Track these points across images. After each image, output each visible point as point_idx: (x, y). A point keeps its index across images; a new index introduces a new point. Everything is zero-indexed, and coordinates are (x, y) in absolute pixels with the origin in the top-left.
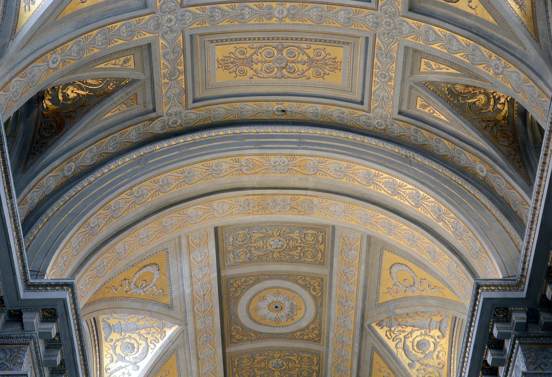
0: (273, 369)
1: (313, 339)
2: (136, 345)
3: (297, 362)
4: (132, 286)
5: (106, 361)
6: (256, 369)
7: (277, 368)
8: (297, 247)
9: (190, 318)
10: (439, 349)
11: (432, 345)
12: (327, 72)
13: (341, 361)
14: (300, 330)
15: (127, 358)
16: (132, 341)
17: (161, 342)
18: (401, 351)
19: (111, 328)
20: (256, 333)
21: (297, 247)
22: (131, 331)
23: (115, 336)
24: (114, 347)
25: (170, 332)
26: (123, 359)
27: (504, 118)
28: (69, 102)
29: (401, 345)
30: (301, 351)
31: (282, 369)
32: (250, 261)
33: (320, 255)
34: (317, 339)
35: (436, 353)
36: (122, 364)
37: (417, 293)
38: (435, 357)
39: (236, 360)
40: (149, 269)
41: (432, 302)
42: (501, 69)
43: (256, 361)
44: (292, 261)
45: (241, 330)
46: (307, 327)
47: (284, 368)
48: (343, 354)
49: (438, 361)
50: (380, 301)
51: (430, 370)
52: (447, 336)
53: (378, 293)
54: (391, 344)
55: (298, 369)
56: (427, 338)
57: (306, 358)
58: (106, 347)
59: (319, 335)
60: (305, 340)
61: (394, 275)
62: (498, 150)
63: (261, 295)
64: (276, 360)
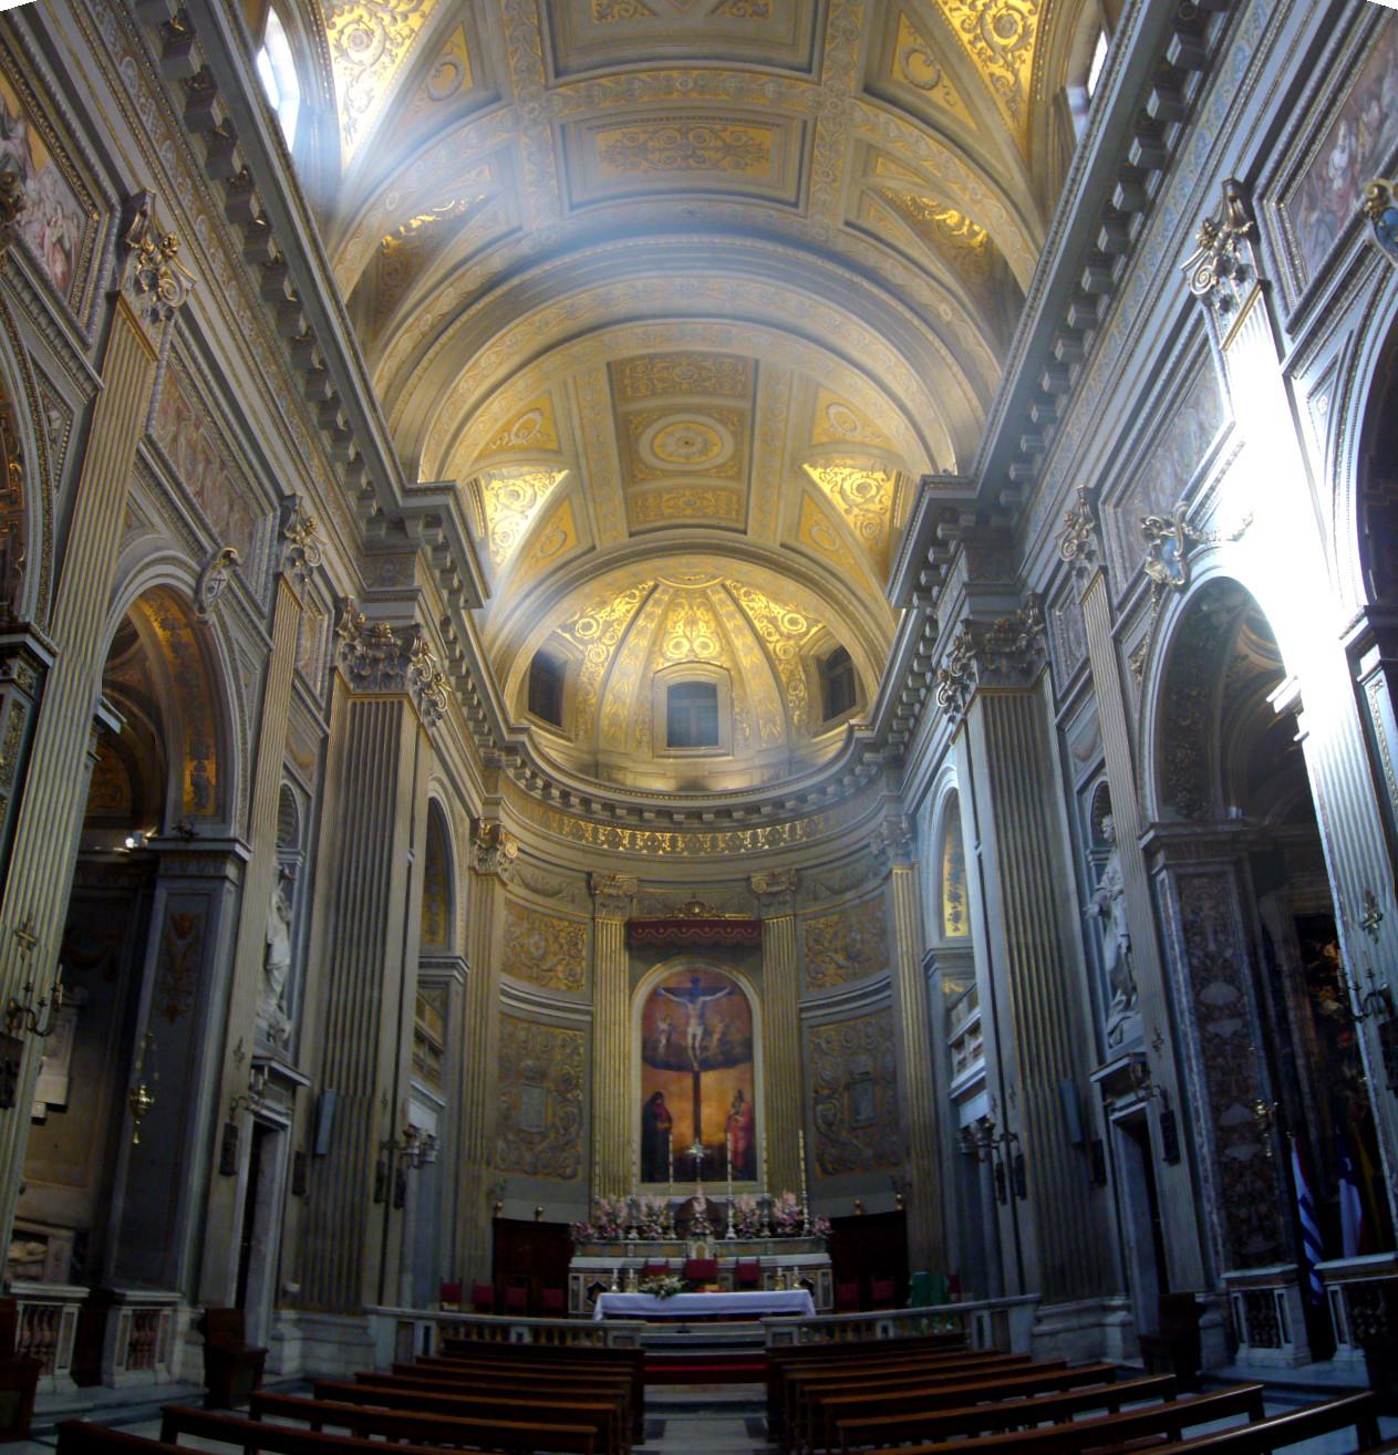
2: (521, 492)
4: (513, 437)
5: (489, 511)
8: (710, 378)
9: (583, 462)
10: (882, 492)
11: (874, 489)
12: (750, 162)
14: (716, 467)
15: (513, 507)
16: (517, 488)
17: (551, 488)
18: (839, 497)
19: (491, 477)
20: (662, 471)
21: (710, 378)
22: (514, 478)
23: (496, 484)
24: (497, 496)
25: (560, 477)
26: (508, 507)
27: (981, 244)
28: (413, 234)
29: (837, 489)
32: (654, 394)
33: (740, 386)
34: (738, 477)
36: (509, 513)
37: (858, 438)
38: (877, 500)
40: (530, 415)
41: (876, 452)
42: (979, 197)
44: (705, 392)
46: (725, 464)
50: (814, 442)
51: (870, 515)
52: (893, 480)
53: (811, 433)
54: (826, 488)
56: (869, 481)
58: (488, 497)
59: (739, 473)
61: (832, 416)
62: (968, 291)
63: (669, 430)
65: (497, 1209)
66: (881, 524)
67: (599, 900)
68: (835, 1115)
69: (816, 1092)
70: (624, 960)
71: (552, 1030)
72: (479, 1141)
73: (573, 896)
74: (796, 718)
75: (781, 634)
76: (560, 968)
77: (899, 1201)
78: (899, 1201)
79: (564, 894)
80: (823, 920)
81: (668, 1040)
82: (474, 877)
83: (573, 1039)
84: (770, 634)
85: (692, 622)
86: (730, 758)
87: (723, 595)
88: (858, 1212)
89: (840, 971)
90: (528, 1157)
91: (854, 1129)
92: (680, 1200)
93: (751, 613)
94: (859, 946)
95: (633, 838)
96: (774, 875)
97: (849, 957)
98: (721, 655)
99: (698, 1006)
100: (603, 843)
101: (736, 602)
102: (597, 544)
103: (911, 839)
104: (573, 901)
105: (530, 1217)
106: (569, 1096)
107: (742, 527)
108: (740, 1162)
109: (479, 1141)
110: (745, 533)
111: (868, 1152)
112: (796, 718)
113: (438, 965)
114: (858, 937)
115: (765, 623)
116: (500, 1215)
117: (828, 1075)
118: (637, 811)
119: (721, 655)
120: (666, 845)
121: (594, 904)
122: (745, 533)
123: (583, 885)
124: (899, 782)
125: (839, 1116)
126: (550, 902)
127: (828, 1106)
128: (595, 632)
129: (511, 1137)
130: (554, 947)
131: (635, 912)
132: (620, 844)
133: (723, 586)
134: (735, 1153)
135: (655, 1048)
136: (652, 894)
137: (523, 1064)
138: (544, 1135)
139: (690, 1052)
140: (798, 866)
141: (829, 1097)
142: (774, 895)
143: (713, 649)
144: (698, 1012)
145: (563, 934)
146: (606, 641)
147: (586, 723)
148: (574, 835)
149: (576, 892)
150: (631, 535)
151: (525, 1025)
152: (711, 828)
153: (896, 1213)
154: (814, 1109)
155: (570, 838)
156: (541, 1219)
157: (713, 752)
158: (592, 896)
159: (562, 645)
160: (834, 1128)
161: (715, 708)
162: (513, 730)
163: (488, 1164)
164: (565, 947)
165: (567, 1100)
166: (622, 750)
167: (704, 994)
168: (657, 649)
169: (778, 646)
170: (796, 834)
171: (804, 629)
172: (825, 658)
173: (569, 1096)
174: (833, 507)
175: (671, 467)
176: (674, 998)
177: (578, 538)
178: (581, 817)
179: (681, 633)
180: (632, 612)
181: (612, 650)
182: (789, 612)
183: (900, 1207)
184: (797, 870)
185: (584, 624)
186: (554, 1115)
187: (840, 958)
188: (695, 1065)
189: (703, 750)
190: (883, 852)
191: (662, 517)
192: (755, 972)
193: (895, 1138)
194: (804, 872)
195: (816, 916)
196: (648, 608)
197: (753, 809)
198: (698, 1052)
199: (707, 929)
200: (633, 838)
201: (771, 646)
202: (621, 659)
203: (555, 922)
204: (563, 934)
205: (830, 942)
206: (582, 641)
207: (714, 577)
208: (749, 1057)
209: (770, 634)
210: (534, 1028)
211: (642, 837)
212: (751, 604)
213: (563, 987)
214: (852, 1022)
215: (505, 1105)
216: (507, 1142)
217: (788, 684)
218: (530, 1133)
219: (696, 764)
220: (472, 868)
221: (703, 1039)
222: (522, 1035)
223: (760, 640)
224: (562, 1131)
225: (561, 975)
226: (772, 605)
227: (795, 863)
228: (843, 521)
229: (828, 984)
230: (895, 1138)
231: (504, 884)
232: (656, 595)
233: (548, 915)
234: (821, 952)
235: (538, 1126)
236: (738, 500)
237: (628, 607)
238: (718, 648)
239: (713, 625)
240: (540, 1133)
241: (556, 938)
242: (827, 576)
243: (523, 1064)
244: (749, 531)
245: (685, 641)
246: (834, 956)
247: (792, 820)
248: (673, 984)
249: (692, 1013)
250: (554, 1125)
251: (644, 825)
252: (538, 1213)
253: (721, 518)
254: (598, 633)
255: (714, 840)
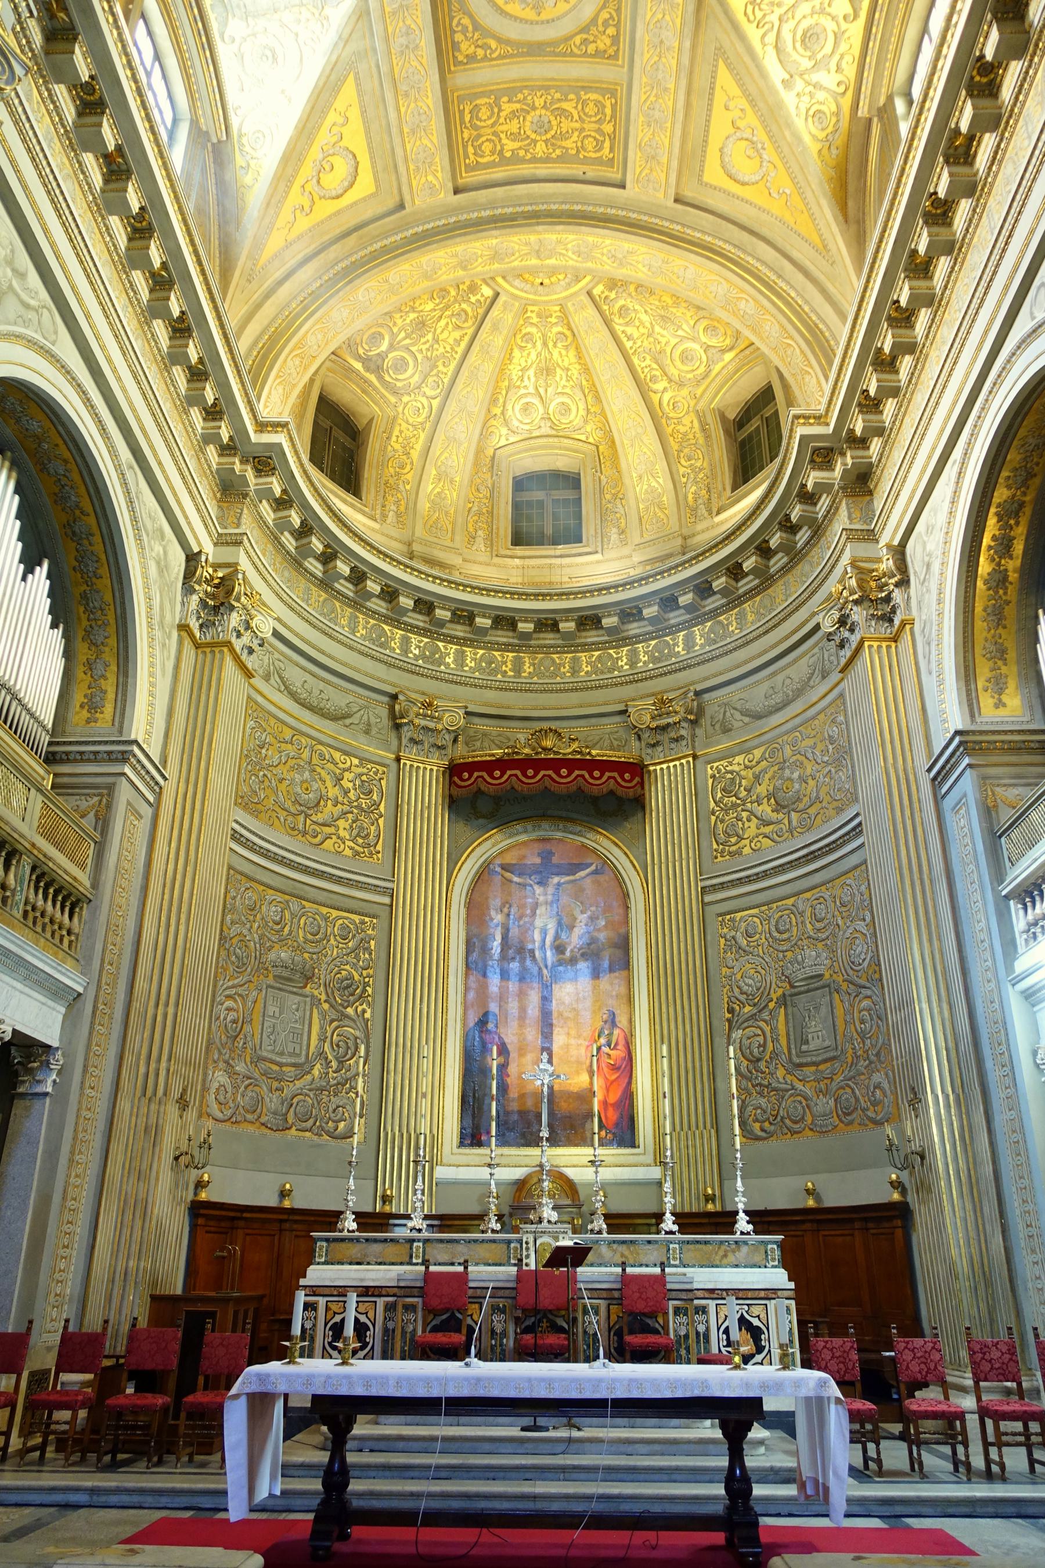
0: (533, 136)
1: (605, 51)
3: (576, 117)
6: (503, 136)
7: (540, 134)
10: (843, 47)
13: (656, 96)
18: (771, 51)
29: (771, 38)
30: (583, 88)
31: (549, 136)
35: (836, 57)
38: (833, 66)
39: (467, 111)
43: (503, 114)
45: (470, 28)
46: (594, 21)
47: (553, 132)
48: (660, 77)
49: (839, 77)
51: (821, 95)
54: (753, 34)
55: (576, 134)
57: (591, 105)
59: (615, 40)
60: (592, 56)
64: (538, 112)
65: (200, 1185)
66: (837, 114)
67: (407, 733)
68: (764, 1045)
69: (731, 1011)
70: (439, 820)
71: (324, 910)
72: (164, 1064)
73: (369, 725)
74: (690, 497)
75: (670, 381)
76: (341, 823)
77: (898, 1185)
78: (898, 1185)
79: (355, 719)
80: (739, 759)
81: (505, 938)
82: (187, 643)
83: (360, 928)
84: (654, 379)
85: (547, 371)
86: (598, 557)
87: (591, 311)
88: (811, 1203)
89: (767, 830)
90: (272, 1101)
91: (800, 1065)
92: (518, 1173)
93: (628, 344)
94: (797, 786)
95: (460, 658)
96: (663, 702)
97: (779, 807)
98: (586, 422)
99: (551, 890)
100: (416, 658)
101: (608, 323)
102: (407, 198)
103: (897, 585)
104: (367, 732)
105: (272, 1201)
106: (350, 1011)
107: (615, 175)
108: (612, 1115)
109: (164, 1064)
110: (624, 187)
111: (824, 1104)
112: (690, 497)
113: (95, 758)
114: (796, 775)
115: (648, 362)
116: (203, 1196)
117: (749, 985)
118: (464, 615)
119: (586, 422)
120: (508, 668)
121: (400, 739)
122: (624, 187)
123: (384, 712)
124: (868, 514)
125: (770, 1046)
126: (329, 727)
127: (749, 1031)
128: (411, 376)
129: (240, 1068)
130: (333, 792)
131: (461, 752)
132: (440, 662)
133: (589, 294)
134: (604, 1103)
135: (485, 950)
136: (485, 735)
137: (272, 956)
138: (303, 1068)
139: (537, 954)
140: (699, 687)
141: (753, 1017)
142: (664, 728)
143: (576, 416)
144: (550, 898)
145: (346, 775)
146: (430, 393)
147: (397, 503)
148: (372, 640)
149: (373, 720)
150: (457, 191)
151: (280, 897)
152: (571, 644)
153: (891, 1206)
154: (729, 1037)
155: (367, 643)
156: (287, 1204)
157: (574, 551)
158: (397, 727)
159: (364, 391)
160: (762, 1065)
161: (578, 501)
162: (262, 426)
163: (183, 1104)
164: (352, 795)
165: (348, 1017)
166: (448, 543)
167: (557, 874)
168: (497, 411)
169: (666, 397)
170: (695, 644)
171: (702, 369)
172: (732, 415)
173: (350, 1011)
174: (763, 74)
175: (513, 32)
176: (516, 879)
177: (376, 180)
178: (387, 619)
179: (532, 390)
180: (463, 345)
181: (435, 403)
182: (682, 339)
183: (896, 1196)
184: (697, 694)
185: (395, 358)
186: (322, 1039)
187: (766, 809)
188: (545, 971)
189: (561, 549)
190: (842, 621)
191: (504, 161)
192: (636, 842)
193: (877, 1078)
194: (706, 696)
195: (728, 755)
196: (483, 334)
197: (630, 612)
198: (549, 954)
199: (564, 772)
200: (460, 658)
201: (655, 398)
202: (446, 417)
203: (337, 755)
204: (346, 775)
205: (748, 790)
206: (395, 392)
207: (578, 280)
208: (623, 962)
209: (654, 379)
210: (294, 905)
211: (472, 656)
212: (629, 330)
213: (348, 852)
214: (790, 902)
215: (232, 1015)
216: (231, 1073)
217: (679, 451)
218: (280, 1065)
219: (550, 566)
220: (183, 627)
221: (557, 937)
222: (272, 912)
223: (643, 389)
224: (334, 1064)
225: (343, 833)
226: (657, 329)
227: (693, 683)
228: (780, 105)
229: (747, 851)
230: (877, 1078)
231: (248, 674)
232: (495, 312)
233: (321, 743)
234: (734, 806)
235: (293, 1054)
236: (614, 107)
237: (457, 334)
238: (582, 412)
239: (575, 371)
240: (294, 1065)
241: (339, 780)
242: (745, 236)
243: (272, 956)
244: (628, 185)
245: (536, 401)
246: (759, 810)
247: (688, 625)
248: (510, 858)
249: (541, 899)
250: (321, 1054)
251: (476, 638)
252: (283, 1194)
253: (586, 161)
254: (416, 378)
255: (575, 661)
